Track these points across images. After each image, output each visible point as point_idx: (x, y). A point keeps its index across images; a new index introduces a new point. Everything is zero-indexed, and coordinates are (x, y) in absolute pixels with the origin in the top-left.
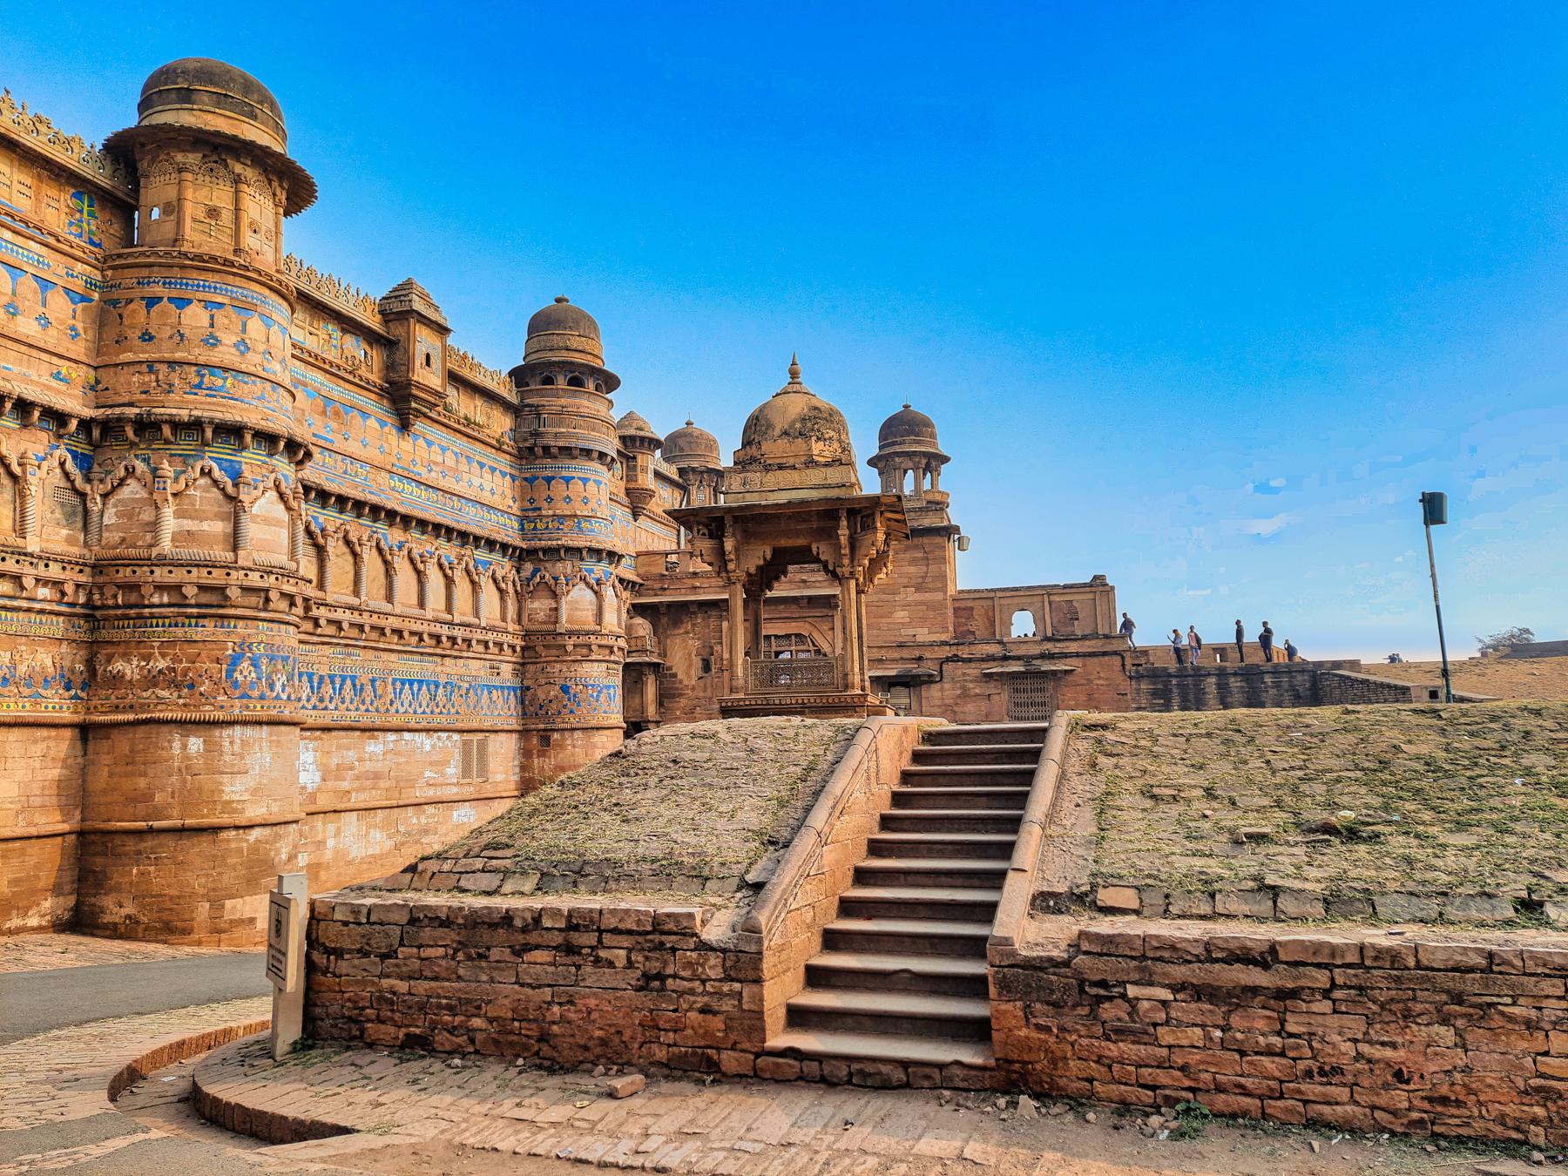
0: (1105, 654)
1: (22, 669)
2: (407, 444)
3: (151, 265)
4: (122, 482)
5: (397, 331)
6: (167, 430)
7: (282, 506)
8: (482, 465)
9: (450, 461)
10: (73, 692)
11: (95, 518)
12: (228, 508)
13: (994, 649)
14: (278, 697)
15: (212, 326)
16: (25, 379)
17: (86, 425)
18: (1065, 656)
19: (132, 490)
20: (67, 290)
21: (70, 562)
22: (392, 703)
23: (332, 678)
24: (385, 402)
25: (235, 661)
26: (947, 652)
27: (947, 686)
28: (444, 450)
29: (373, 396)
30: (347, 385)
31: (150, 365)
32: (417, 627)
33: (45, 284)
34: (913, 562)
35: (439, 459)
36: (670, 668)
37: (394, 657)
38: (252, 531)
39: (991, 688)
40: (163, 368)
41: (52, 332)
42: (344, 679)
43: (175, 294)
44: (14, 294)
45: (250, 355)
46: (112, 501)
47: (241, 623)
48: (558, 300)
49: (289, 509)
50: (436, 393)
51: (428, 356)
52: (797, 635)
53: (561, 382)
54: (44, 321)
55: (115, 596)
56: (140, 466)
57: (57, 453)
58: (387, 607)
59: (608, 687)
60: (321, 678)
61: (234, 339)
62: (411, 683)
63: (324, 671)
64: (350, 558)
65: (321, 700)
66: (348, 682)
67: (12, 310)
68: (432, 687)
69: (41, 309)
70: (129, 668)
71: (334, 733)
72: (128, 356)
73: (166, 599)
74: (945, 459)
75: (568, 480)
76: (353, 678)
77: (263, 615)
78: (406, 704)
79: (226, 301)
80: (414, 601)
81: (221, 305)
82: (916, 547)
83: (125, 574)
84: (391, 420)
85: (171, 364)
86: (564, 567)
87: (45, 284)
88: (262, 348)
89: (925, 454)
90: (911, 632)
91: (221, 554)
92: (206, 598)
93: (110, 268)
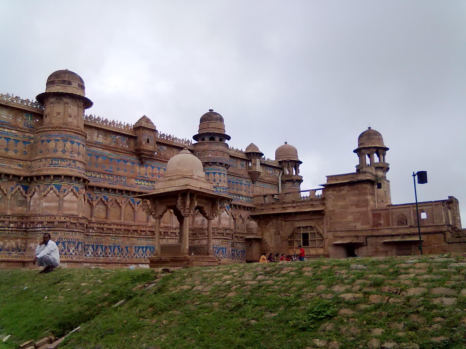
1: (6, 246)
2: (143, 169)
3: (43, 131)
4: (34, 193)
5: (138, 132)
6: (42, 178)
7: (75, 197)
10: (21, 252)
11: (28, 203)
12: (58, 198)
14: (71, 254)
15: (56, 146)
16: (10, 168)
17: (26, 178)
19: (36, 195)
20: (23, 142)
21: (20, 217)
22: (134, 254)
23: (110, 247)
24: (134, 156)
27: (369, 247)
28: (159, 169)
29: (129, 155)
30: (118, 153)
31: (41, 159)
32: (143, 229)
34: (354, 195)
35: (157, 172)
36: (265, 240)
37: (135, 239)
38: (66, 205)
40: (43, 160)
41: (18, 153)
42: (115, 247)
43: (47, 139)
44: (7, 145)
45: (66, 153)
46: (32, 199)
47: (59, 232)
48: (210, 110)
49: (77, 197)
50: (151, 151)
51: (148, 140)
52: (311, 227)
53: (207, 139)
54: (16, 151)
55: (30, 225)
56: (37, 188)
57: (18, 187)
58: (132, 223)
59: (222, 248)
60: (106, 247)
61: (62, 149)
62: (143, 248)
63: (107, 245)
64: (119, 208)
65: (106, 254)
66: (117, 248)
67: (7, 150)
68: (152, 249)
69: (15, 148)
71: (110, 265)
72: (37, 158)
73: (40, 226)
74: (388, 149)
76: (118, 247)
77: (66, 230)
78: (141, 255)
79: (60, 138)
80: (145, 220)
81: (59, 140)
83: (32, 219)
84: (137, 161)
85: (46, 158)
87: (17, 141)
88: (70, 150)
89: (375, 148)
90: (354, 224)
91: (55, 213)
92: (50, 225)
93: (36, 133)
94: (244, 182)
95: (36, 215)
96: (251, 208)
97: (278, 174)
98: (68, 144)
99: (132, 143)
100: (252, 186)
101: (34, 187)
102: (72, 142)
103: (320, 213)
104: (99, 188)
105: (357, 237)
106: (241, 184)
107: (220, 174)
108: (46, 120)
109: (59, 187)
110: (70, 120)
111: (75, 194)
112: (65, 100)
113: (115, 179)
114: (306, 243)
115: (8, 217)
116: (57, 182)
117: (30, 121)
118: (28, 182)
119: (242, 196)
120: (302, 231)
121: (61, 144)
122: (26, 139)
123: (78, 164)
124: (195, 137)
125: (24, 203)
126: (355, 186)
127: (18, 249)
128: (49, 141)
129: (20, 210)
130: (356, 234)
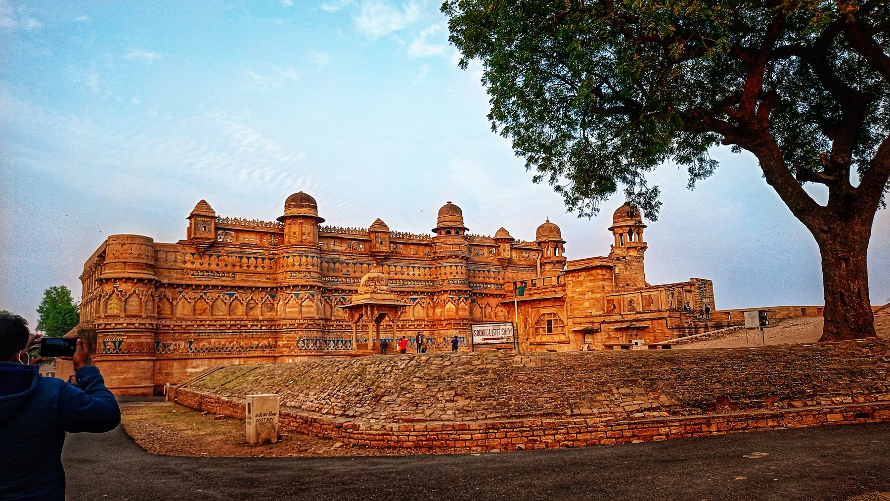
0: (660, 319)
5: (373, 236)
8: (414, 267)
9: (399, 269)
13: (618, 318)
17: (272, 288)
18: (645, 320)
19: (281, 302)
25: (298, 341)
26: (602, 319)
28: (396, 266)
33: (263, 259)
34: (590, 281)
38: (304, 309)
39: (619, 335)
54: (263, 267)
67: (256, 267)
70: (280, 343)
75: (445, 267)
82: (591, 275)
83: (278, 322)
86: (445, 297)
91: (295, 316)
94: (493, 269)
95: (281, 319)
96: (501, 295)
97: (534, 256)
98: (304, 259)
99: (368, 245)
100: (502, 272)
101: (279, 296)
102: (307, 257)
103: (561, 300)
104: (337, 290)
105: (593, 323)
106: (489, 271)
107: (457, 266)
108: (286, 239)
109: (297, 295)
110: (304, 237)
111: (311, 300)
112: (299, 221)
113: (352, 281)
114: (550, 330)
115: (260, 321)
116: (295, 291)
117: (274, 240)
118: (274, 291)
119: (489, 283)
120: (547, 318)
121: (297, 259)
122: (271, 256)
123: (313, 274)
124: (434, 231)
125: (272, 309)
126: (591, 272)
127: (270, 346)
128: (288, 257)
129: (268, 315)
130: (592, 320)
